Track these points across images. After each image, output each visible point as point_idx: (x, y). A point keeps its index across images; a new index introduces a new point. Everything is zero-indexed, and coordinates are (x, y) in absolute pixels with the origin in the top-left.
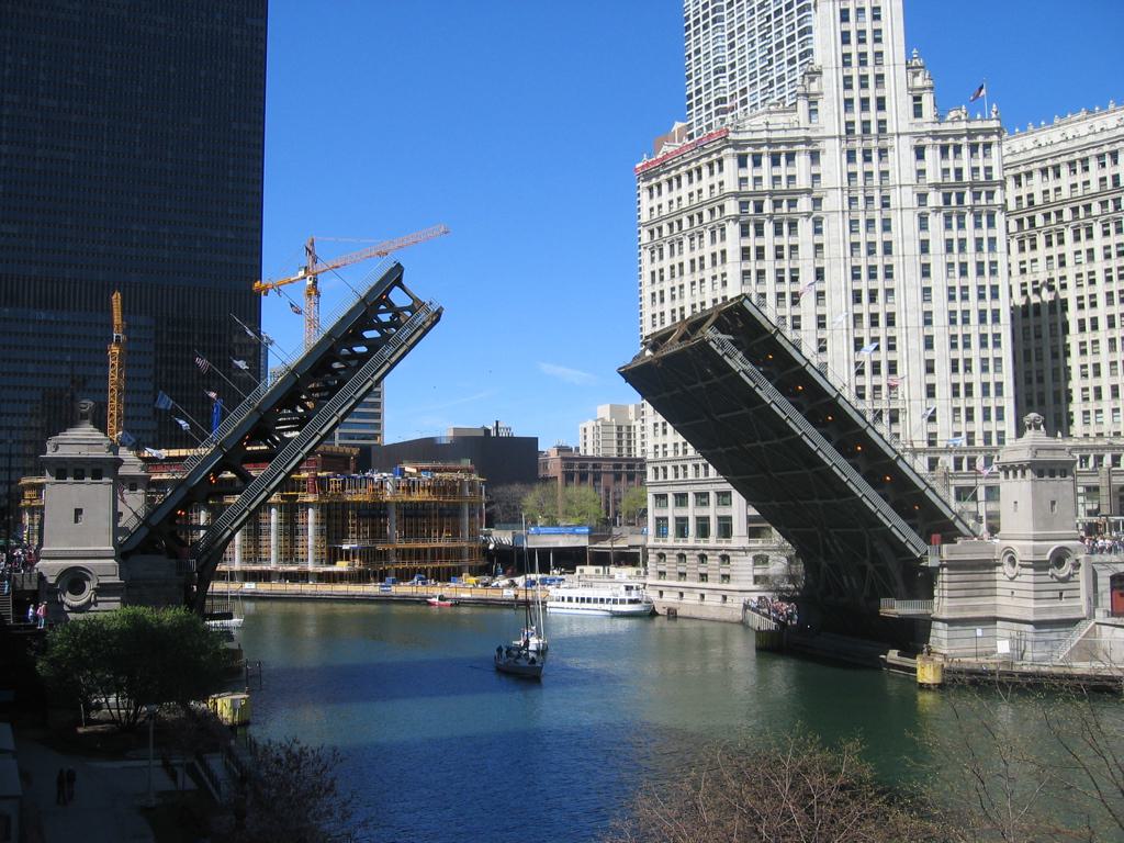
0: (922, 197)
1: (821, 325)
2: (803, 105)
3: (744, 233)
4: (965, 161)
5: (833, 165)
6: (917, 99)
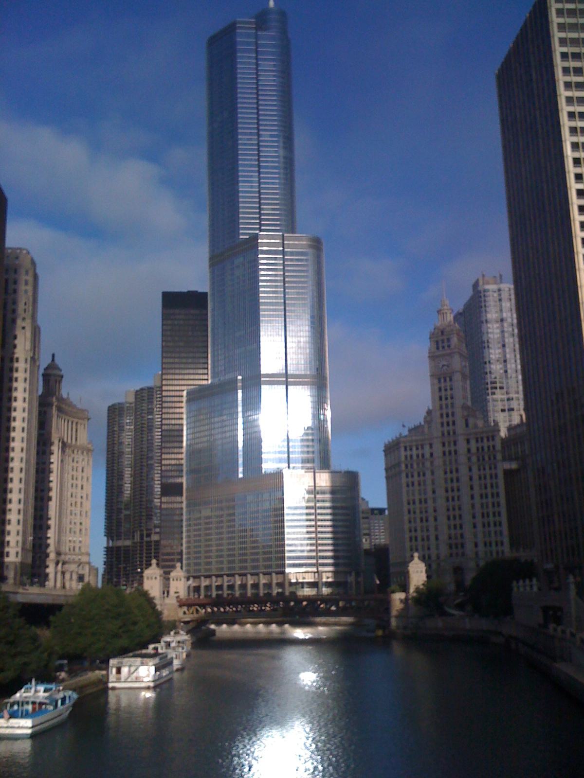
1: (435, 511)
4: (485, 444)
5: (438, 449)
6: (467, 421)
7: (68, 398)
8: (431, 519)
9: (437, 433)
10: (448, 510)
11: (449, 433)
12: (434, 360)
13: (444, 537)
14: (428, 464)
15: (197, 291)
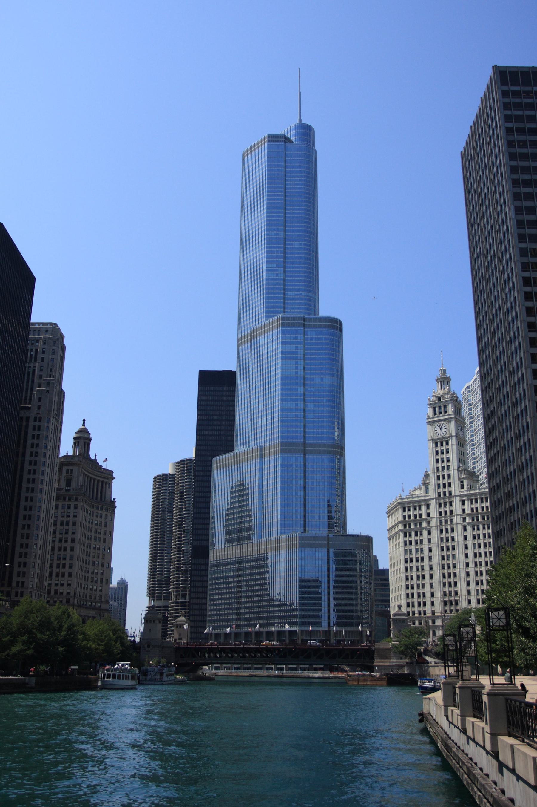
0: (464, 519)
5: (434, 510)
6: (462, 482)
7: (96, 460)
8: (427, 577)
9: (432, 493)
10: (443, 568)
12: (431, 425)
13: (438, 594)
14: (424, 525)
15: (231, 371)
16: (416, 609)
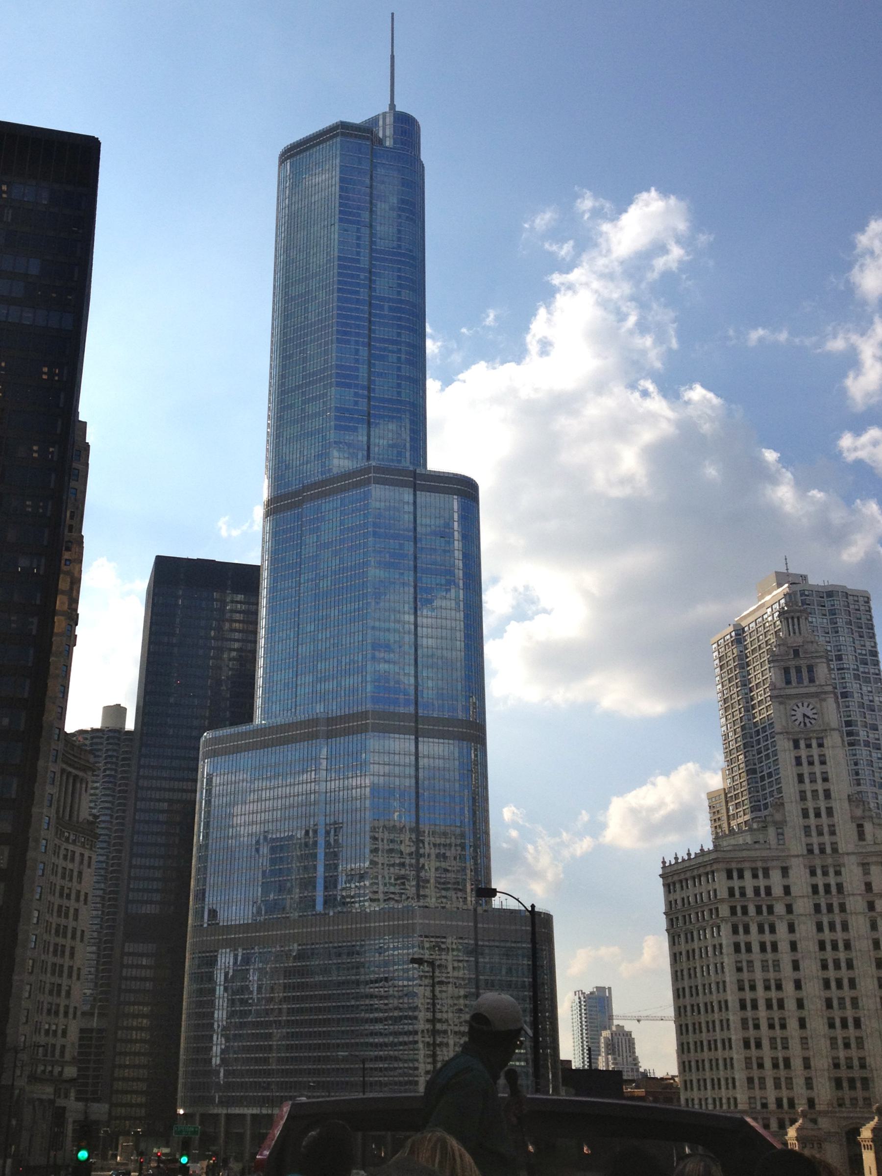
2: (771, 831)
3: (735, 931)
5: (800, 880)
6: (860, 826)
11: (822, 851)
12: (781, 703)
13: (821, 1063)
14: (780, 909)
16: (771, 1095)
